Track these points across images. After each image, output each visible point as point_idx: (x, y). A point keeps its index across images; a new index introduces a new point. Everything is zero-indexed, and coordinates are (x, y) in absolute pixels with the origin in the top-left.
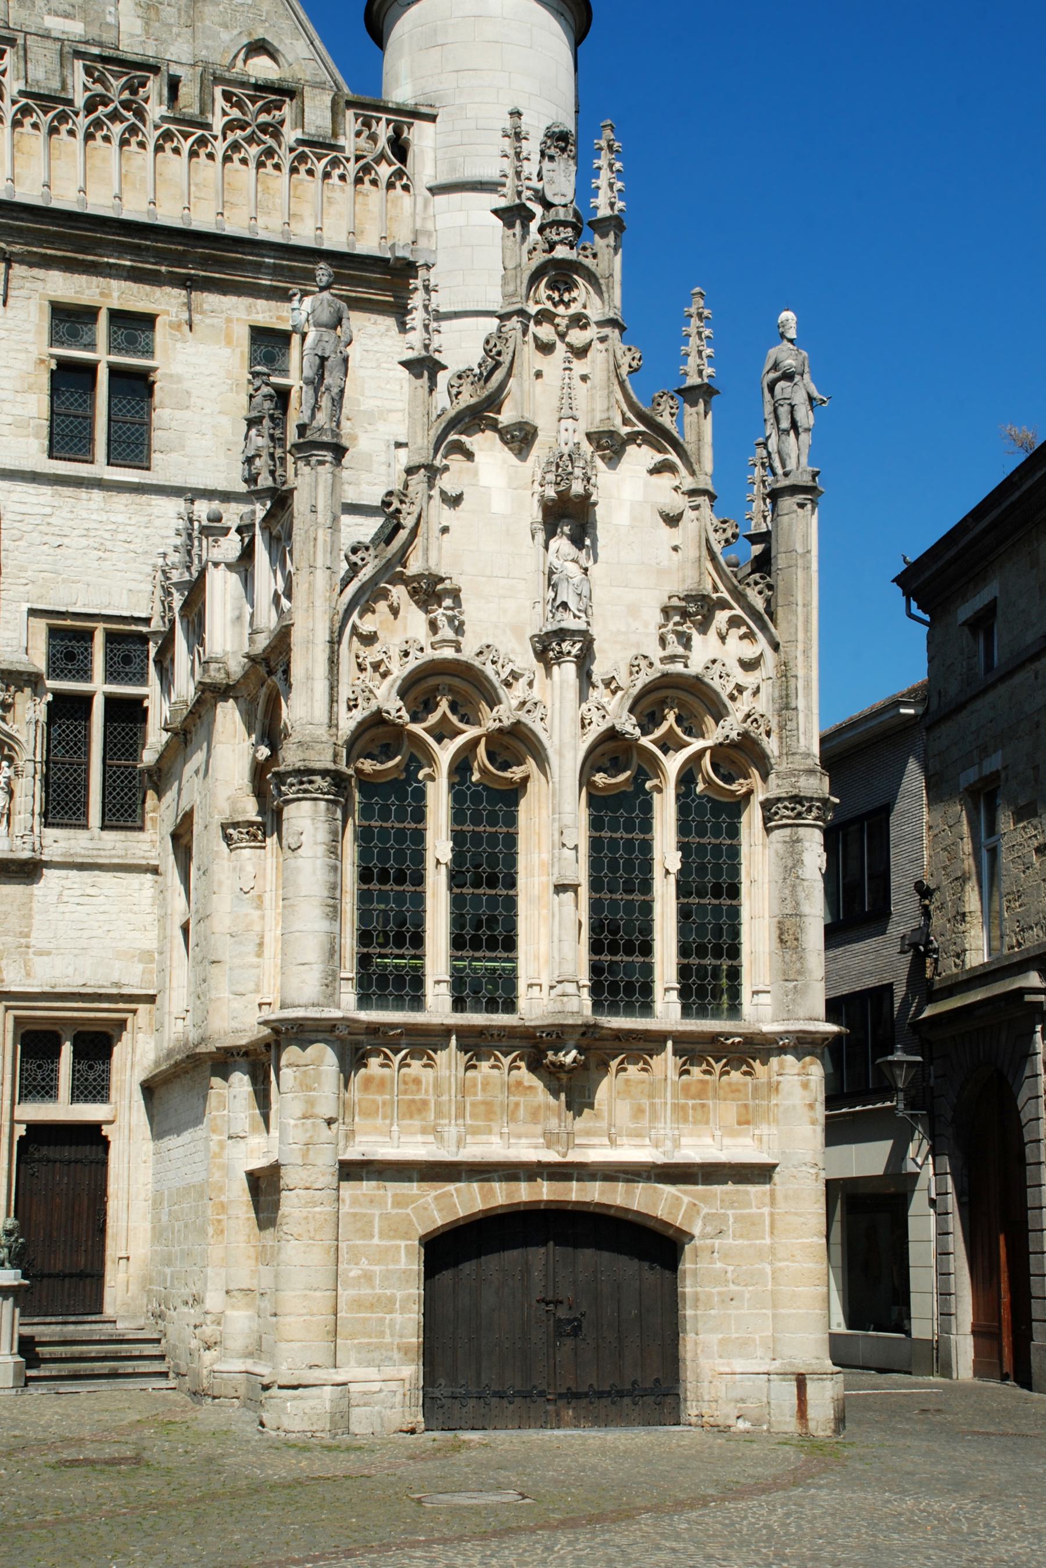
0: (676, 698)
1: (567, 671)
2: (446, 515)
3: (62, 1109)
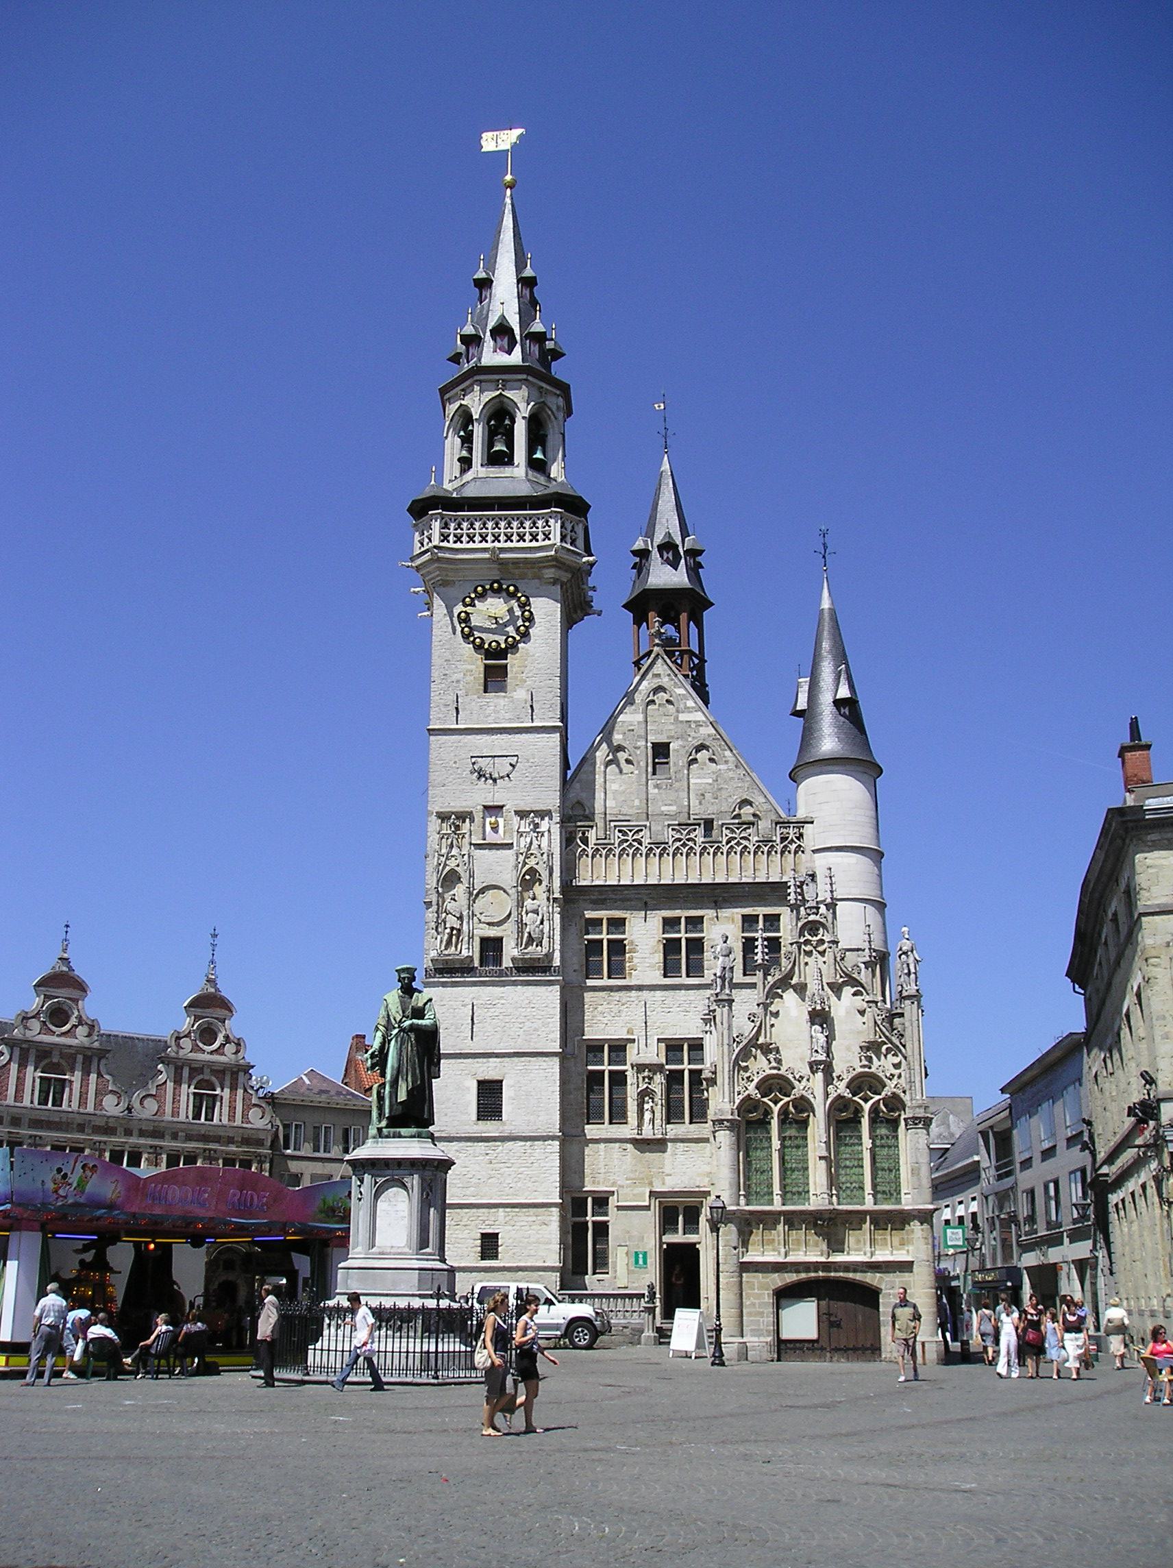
0: (865, 1083)
1: (820, 1075)
2: (773, 1021)
3: (678, 1238)
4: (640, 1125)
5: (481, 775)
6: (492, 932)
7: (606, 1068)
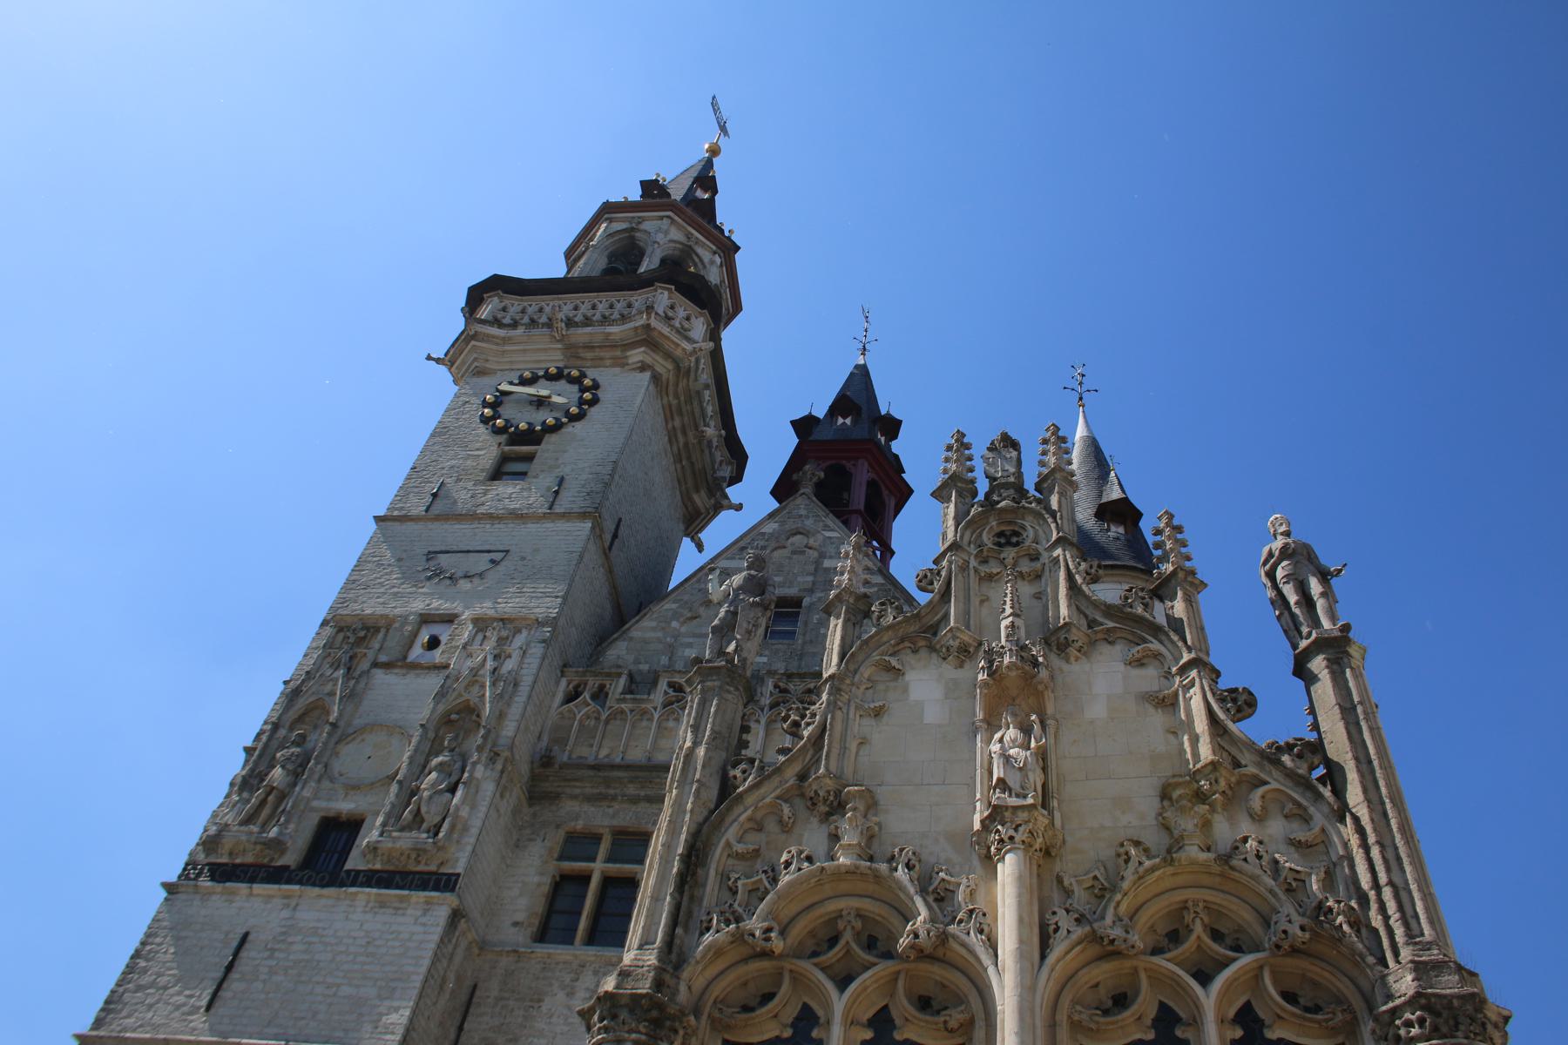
6: (345, 806)
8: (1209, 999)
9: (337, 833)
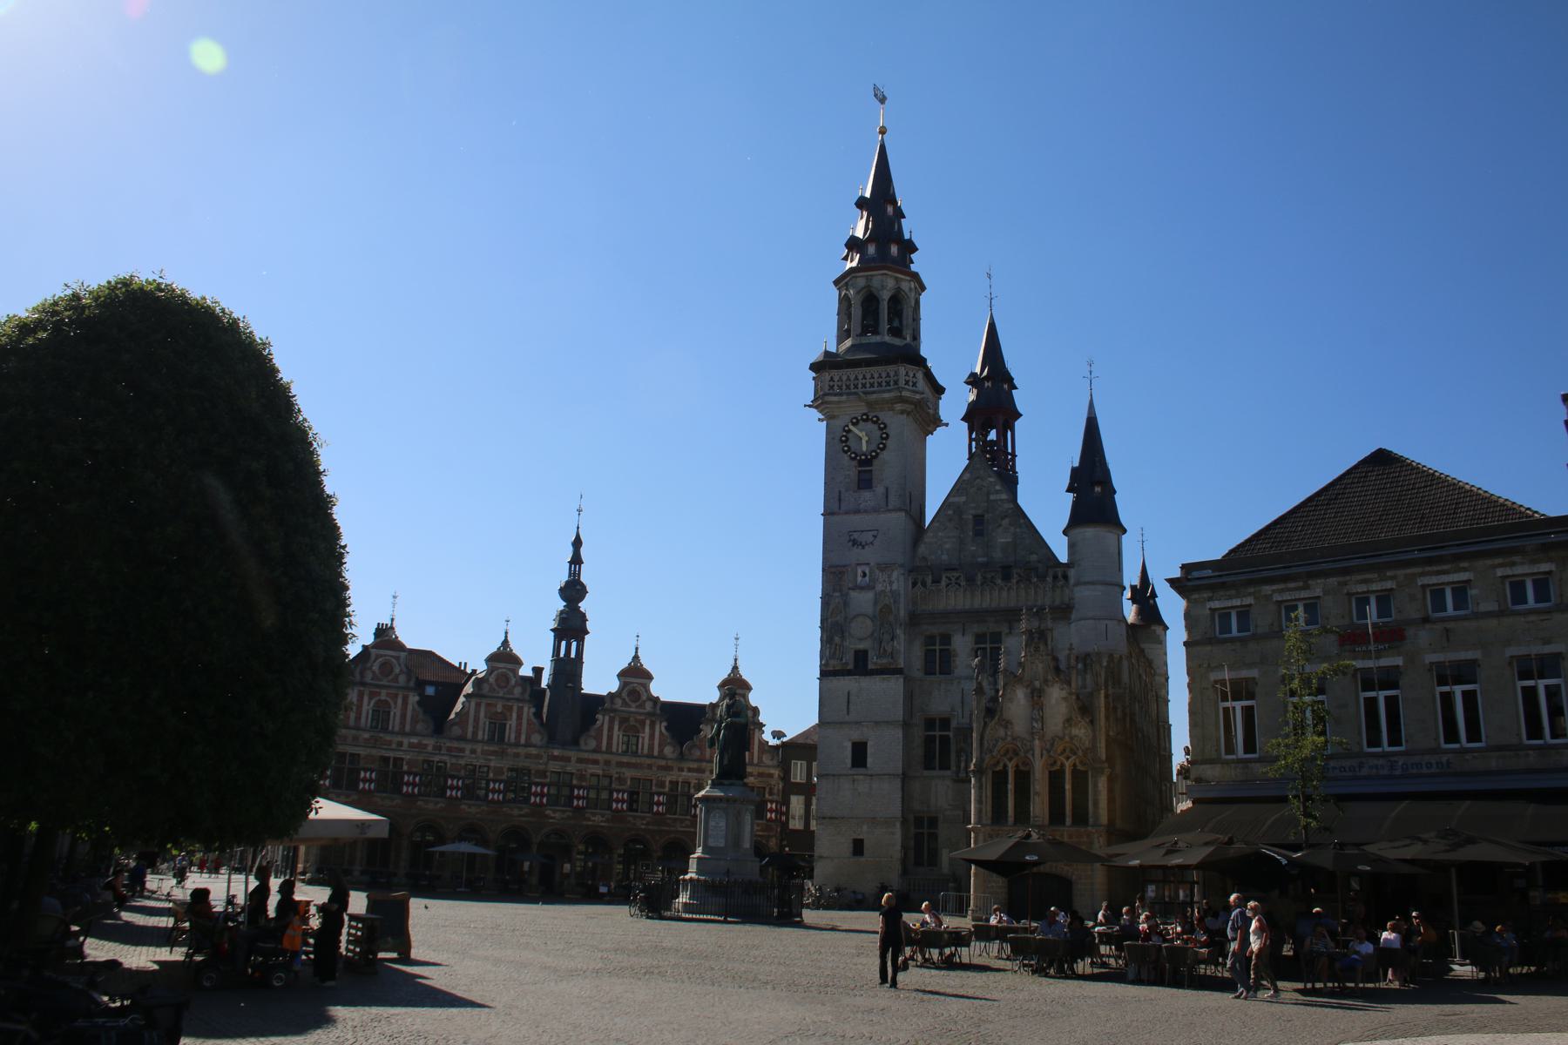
4: (958, 772)
5: (855, 543)
6: (861, 646)
7: (938, 733)
8: (1068, 764)
9: (861, 656)
